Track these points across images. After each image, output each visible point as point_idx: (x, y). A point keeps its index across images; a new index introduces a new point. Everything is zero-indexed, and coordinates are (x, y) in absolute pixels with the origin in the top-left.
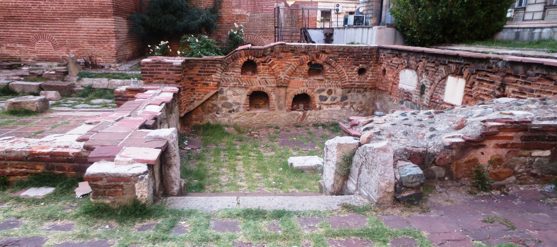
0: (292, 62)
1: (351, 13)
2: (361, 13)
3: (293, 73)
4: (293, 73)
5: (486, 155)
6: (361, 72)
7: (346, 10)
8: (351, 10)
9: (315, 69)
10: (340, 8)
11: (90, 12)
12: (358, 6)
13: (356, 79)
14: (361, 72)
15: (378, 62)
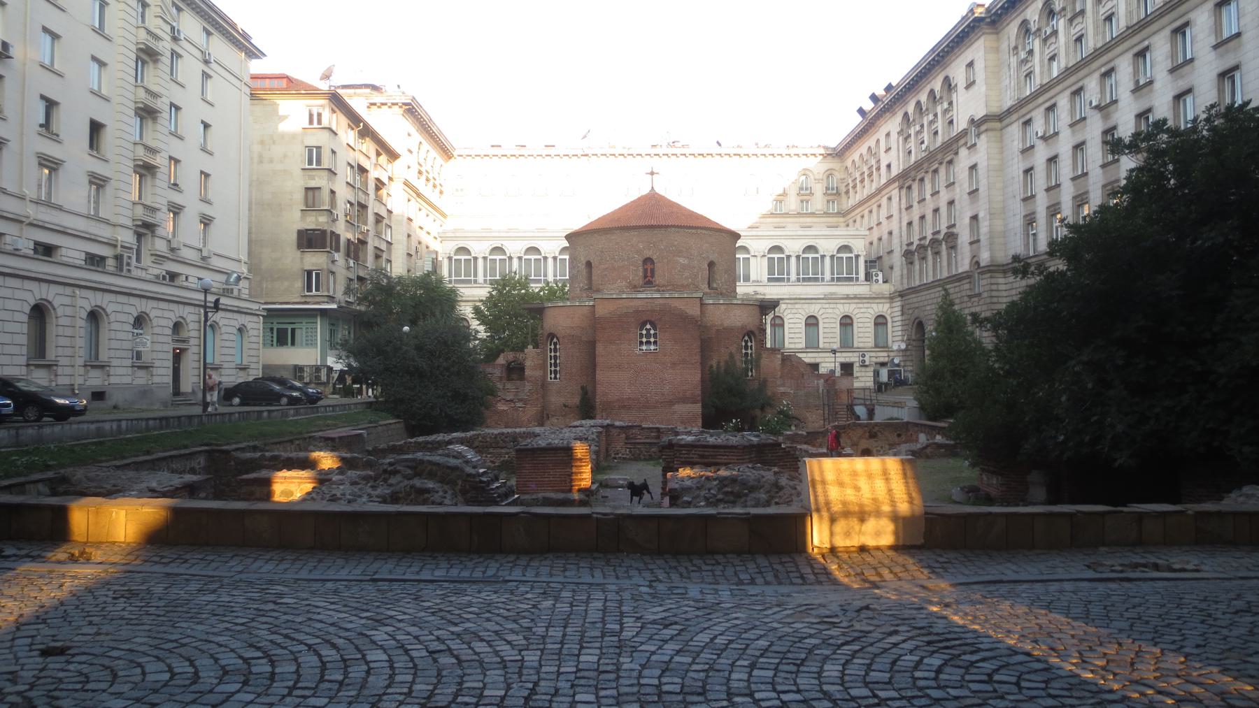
0: (860, 432)
1: (883, 364)
2: (898, 365)
3: (861, 438)
4: (861, 438)
5: (928, 451)
6: (899, 435)
7: (874, 360)
8: (882, 360)
9: (873, 436)
10: (867, 358)
11: (684, 400)
12: (892, 354)
13: (896, 440)
14: (899, 435)
15: (908, 430)
